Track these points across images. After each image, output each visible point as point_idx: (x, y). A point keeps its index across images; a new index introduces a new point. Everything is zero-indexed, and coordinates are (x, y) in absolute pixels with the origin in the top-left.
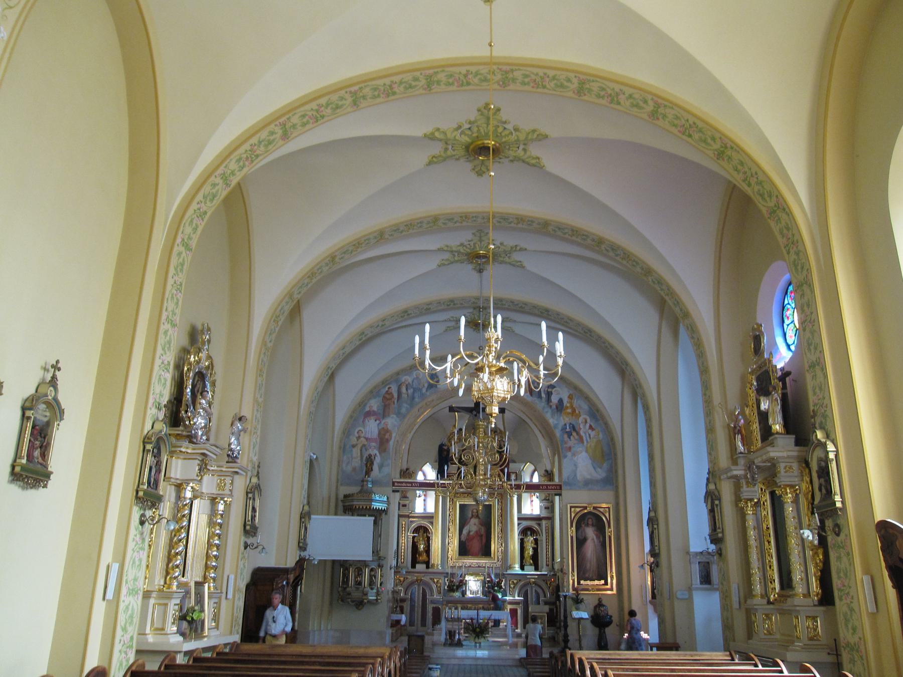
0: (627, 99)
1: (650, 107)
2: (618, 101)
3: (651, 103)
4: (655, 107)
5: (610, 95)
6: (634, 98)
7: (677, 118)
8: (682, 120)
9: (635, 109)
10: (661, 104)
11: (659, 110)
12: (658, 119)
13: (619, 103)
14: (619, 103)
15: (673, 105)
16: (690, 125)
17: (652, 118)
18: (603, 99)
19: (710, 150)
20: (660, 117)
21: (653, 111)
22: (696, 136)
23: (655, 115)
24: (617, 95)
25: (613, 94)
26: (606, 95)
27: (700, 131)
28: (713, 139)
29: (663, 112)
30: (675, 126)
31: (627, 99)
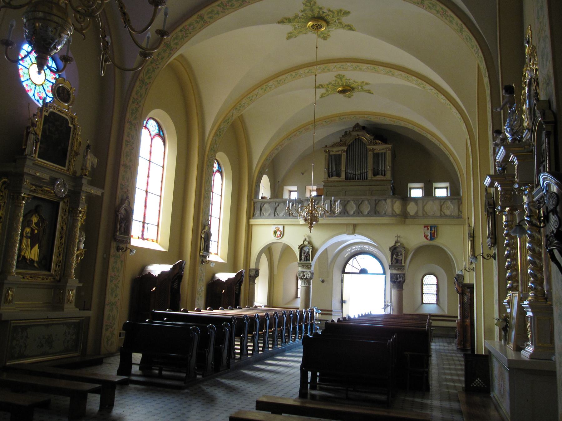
0: (218, 11)
1: (206, 17)
2: (221, 6)
3: (208, 20)
4: (205, 20)
5: (226, 6)
6: (216, 14)
7: (193, 28)
8: (192, 31)
9: (210, 10)
10: (205, 25)
11: (202, 22)
12: (197, 18)
13: (218, 6)
14: (218, 6)
15: (201, 29)
16: (187, 33)
17: (200, 15)
18: (227, 1)
19: (171, 40)
20: (198, 20)
21: (204, 18)
22: (180, 34)
23: (200, 18)
24: (224, 9)
25: (225, 7)
26: (228, 4)
27: (182, 38)
28: (176, 44)
29: (200, 23)
30: (190, 25)
31: (218, 11)
